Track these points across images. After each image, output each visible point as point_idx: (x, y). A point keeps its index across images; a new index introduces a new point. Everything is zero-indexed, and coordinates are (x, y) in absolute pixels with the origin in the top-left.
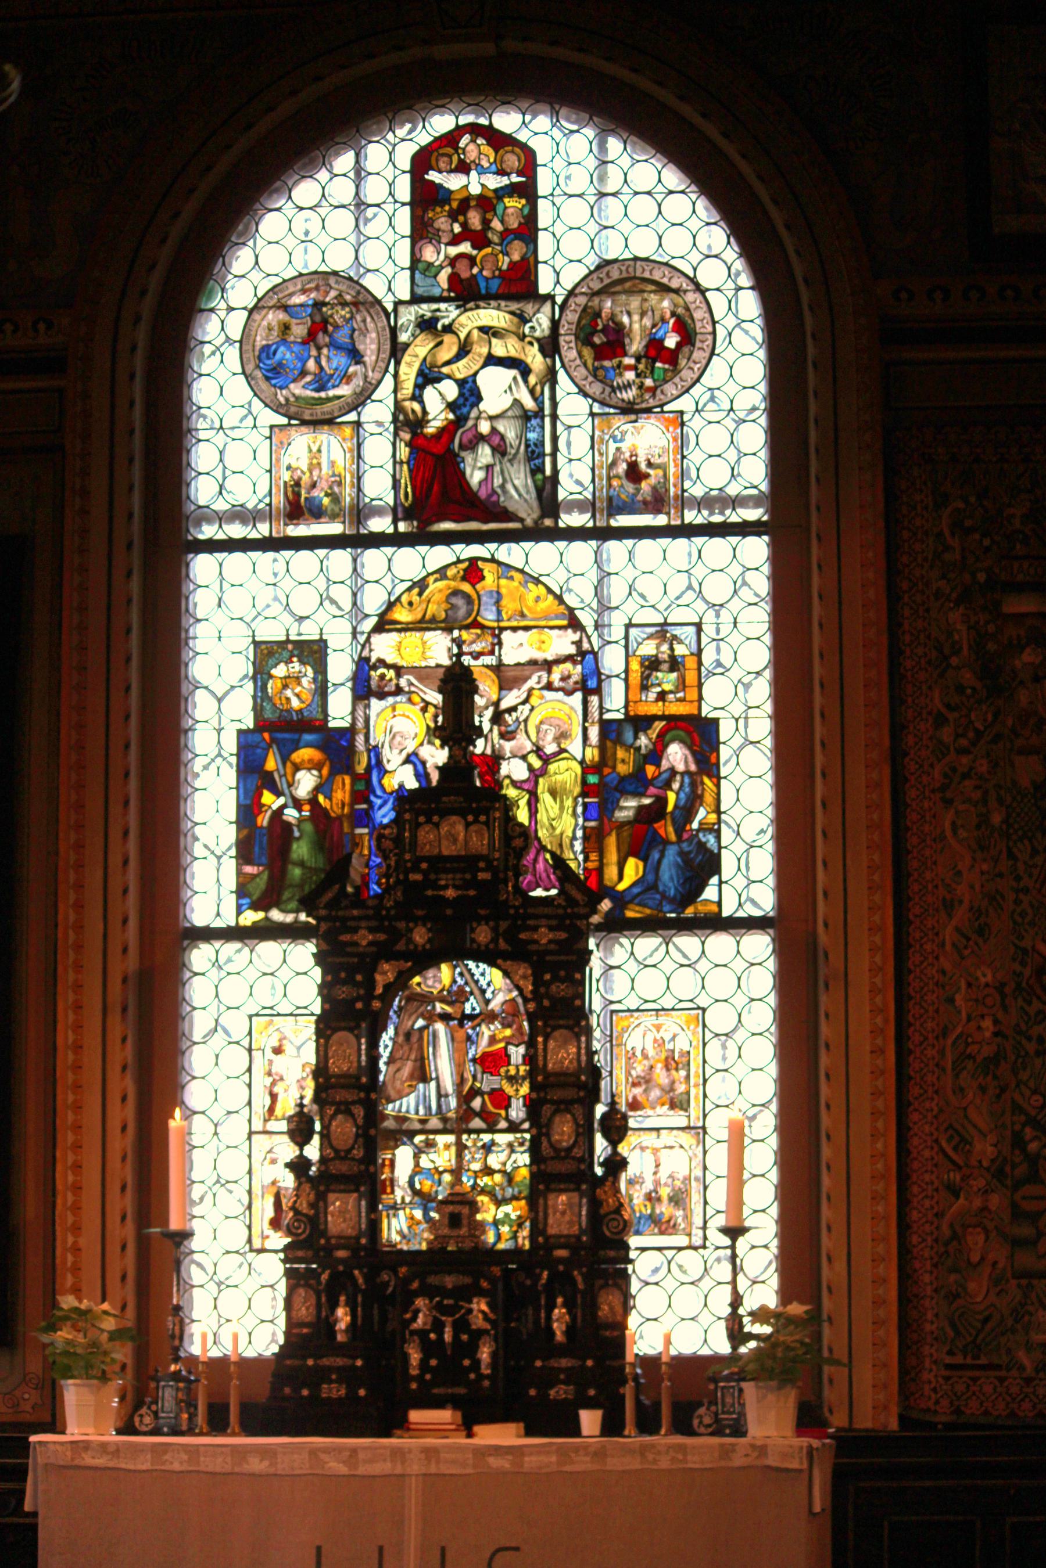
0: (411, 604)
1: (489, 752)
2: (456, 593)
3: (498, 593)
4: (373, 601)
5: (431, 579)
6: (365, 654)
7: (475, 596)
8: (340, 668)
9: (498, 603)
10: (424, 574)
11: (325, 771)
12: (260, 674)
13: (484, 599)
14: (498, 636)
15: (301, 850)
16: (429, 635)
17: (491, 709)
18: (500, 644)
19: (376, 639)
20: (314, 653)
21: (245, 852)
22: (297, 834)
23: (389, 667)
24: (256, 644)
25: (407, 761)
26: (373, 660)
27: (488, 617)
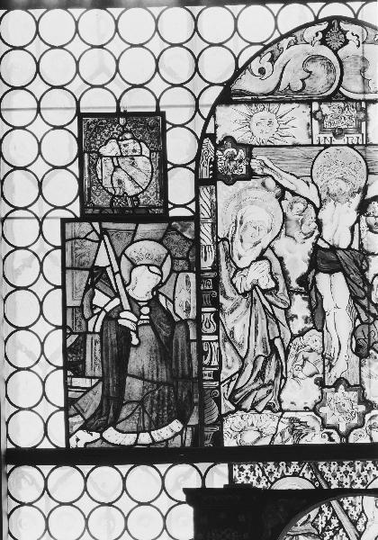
0: (262, 71)
1: (355, 246)
2: (313, 58)
3: (364, 59)
4: (218, 67)
5: (284, 43)
6: (210, 130)
7: (336, 63)
8: (180, 146)
9: (363, 71)
10: (277, 35)
11: (166, 268)
12: (87, 152)
13: (347, 66)
14: (365, 111)
15: (139, 359)
16: (284, 108)
17: (358, 197)
18: (366, 119)
19: (221, 110)
20: (152, 127)
21: (73, 364)
22: (135, 341)
23: (237, 145)
24: (80, 116)
25: (261, 257)
26: (220, 138)
27: (352, 86)
